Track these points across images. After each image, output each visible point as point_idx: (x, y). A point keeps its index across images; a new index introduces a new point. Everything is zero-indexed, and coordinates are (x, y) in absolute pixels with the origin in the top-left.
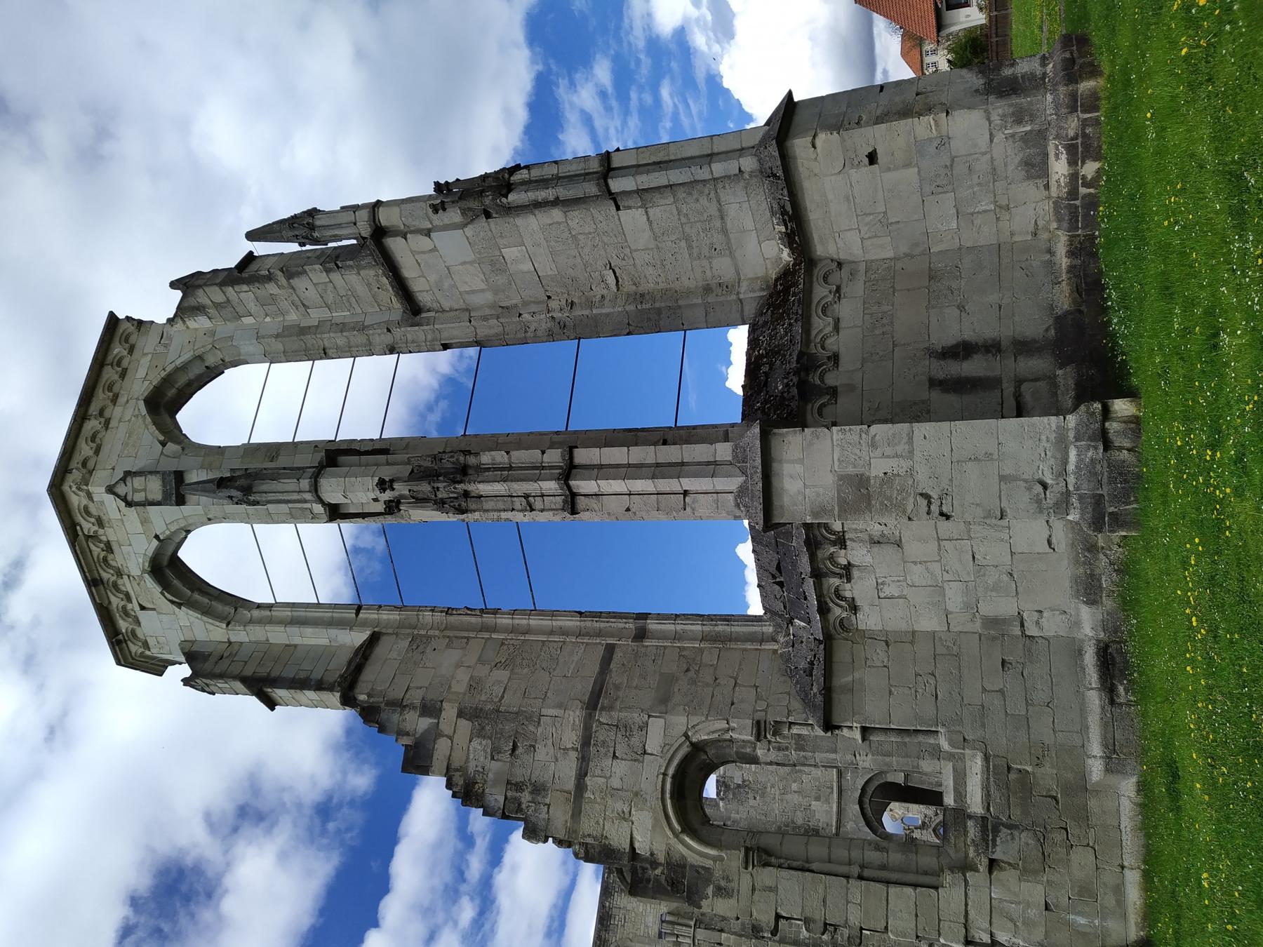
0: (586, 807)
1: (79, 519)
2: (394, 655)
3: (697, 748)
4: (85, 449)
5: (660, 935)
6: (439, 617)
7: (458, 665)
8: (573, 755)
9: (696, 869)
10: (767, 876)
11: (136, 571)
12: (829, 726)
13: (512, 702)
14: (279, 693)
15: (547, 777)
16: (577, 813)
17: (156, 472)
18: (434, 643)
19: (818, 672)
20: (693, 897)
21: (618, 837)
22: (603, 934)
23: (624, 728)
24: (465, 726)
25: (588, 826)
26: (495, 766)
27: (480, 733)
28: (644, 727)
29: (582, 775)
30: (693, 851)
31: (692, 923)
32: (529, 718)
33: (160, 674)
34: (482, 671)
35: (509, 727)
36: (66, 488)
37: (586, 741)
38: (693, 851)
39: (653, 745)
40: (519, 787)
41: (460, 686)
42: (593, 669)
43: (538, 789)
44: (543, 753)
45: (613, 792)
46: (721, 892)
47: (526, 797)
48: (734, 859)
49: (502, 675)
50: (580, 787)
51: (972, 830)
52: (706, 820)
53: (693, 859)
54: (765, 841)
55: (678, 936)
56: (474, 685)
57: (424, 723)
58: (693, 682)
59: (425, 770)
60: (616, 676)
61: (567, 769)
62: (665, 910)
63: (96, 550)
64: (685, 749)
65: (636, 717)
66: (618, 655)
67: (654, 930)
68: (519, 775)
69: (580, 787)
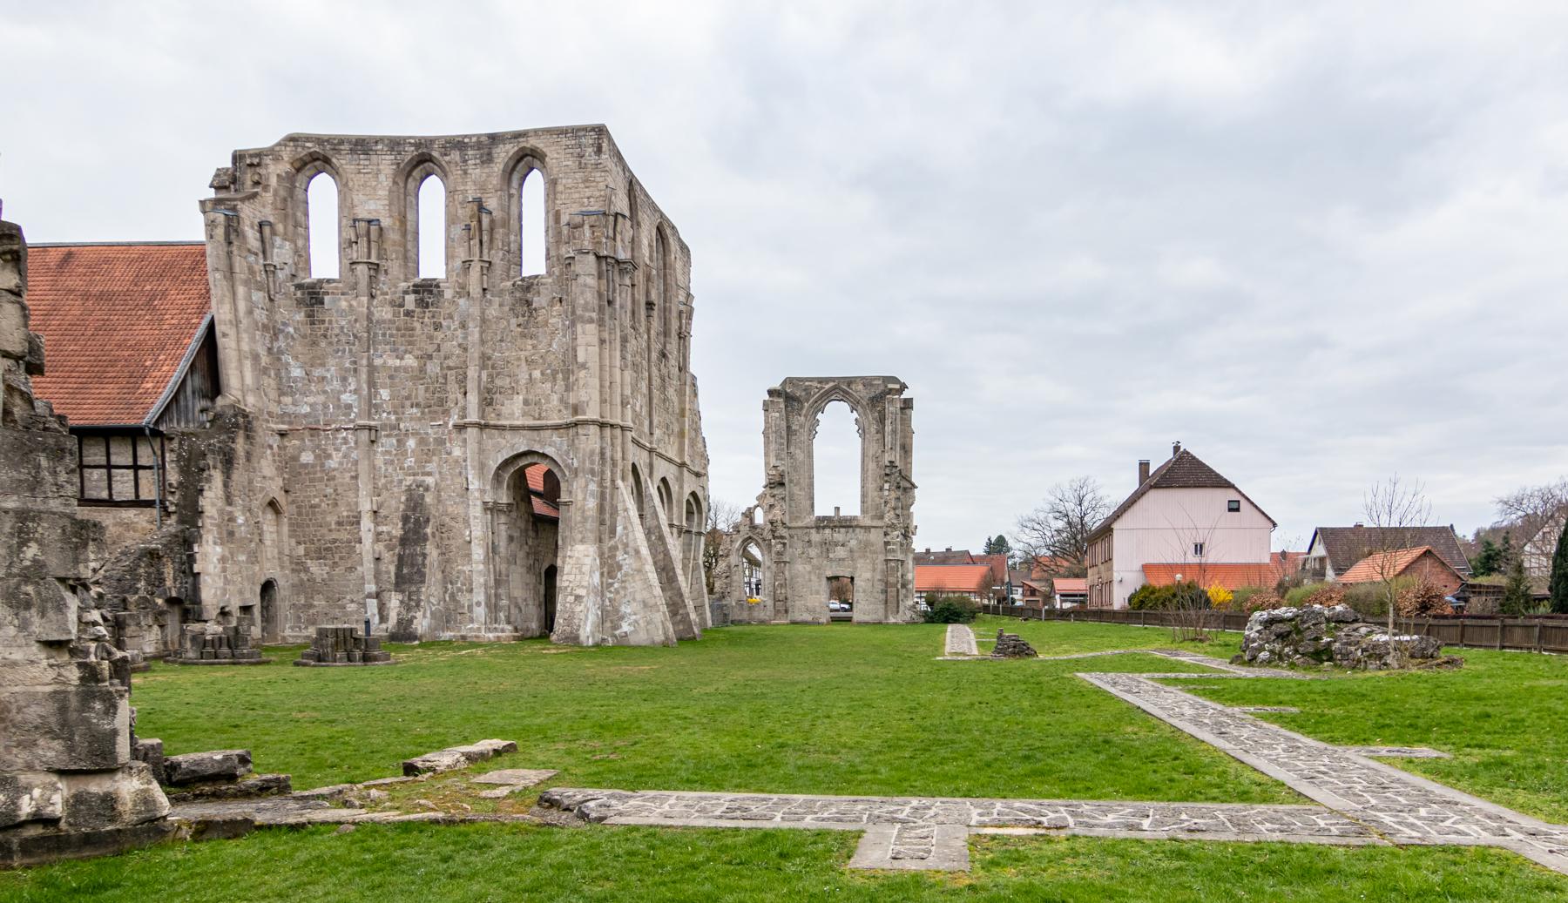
22: (346, 147)
31: (373, 260)
55: (356, 243)
62: (386, 222)
67: (362, 213)
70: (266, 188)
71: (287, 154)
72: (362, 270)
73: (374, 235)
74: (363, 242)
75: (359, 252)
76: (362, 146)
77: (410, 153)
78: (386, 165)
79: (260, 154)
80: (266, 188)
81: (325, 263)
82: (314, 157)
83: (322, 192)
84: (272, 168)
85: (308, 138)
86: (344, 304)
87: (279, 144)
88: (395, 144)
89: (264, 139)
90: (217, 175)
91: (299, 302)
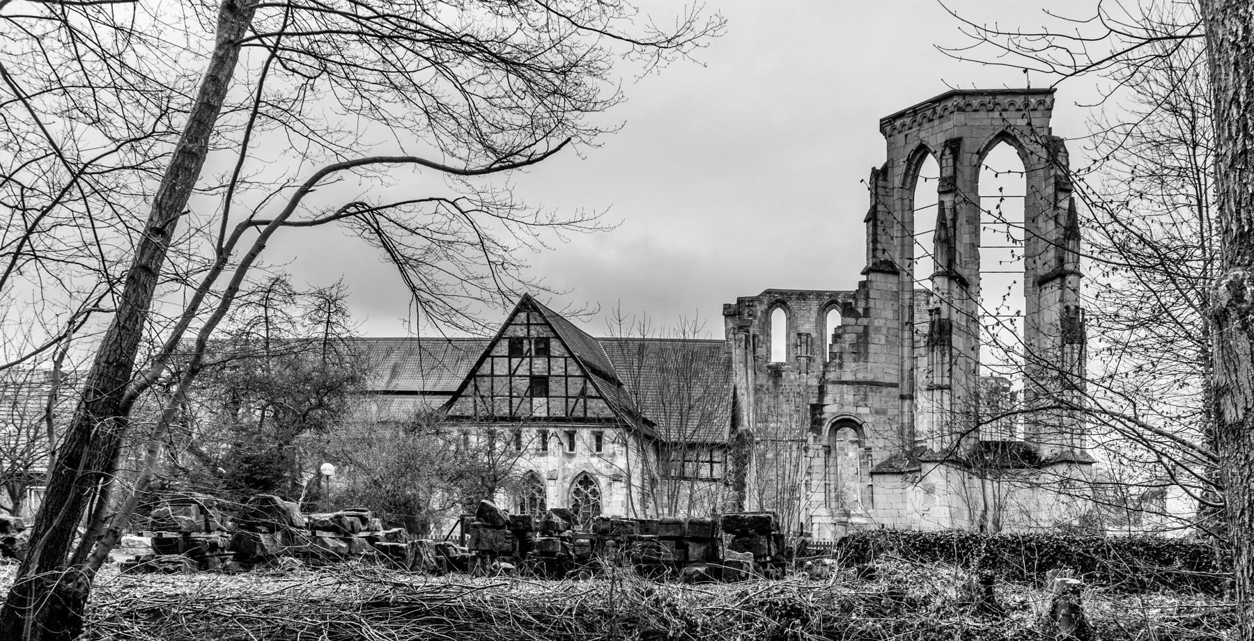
0: (836, 386)
1: (942, 105)
2: (889, 285)
3: (861, 426)
4: (975, 102)
5: (799, 335)
6: (907, 302)
7: (886, 319)
8: (854, 378)
9: (821, 429)
10: (822, 453)
11: (922, 134)
12: (872, 474)
13: (872, 348)
14: (871, 223)
15: (845, 369)
16: (834, 383)
17: (955, 172)
18: (896, 304)
19: (891, 470)
20: (812, 429)
21: (828, 399)
23: (865, 398)
24: (861, 329)
25: (830, 388)
26: (847, 346)
27: (859, 336)
28: (866, 406)
29: (847, 383)
30: (826, 428)
32: (866, 358)
33: (881, 120)
34: (884, 331)
35: (862, 350)
36: (955, 98)
37: (859, 383)
38: (826, 428)
39: (862, 410)
40: (841, 358)
41: (876, 323)
42: (887, 379)
43: (841, 366)
44: (853, 365)
45: (842, 396)
46: (815, 438)
47: (837, 361)
48: (825, 442)
49: (883, 341)
50: (842, 383)
51: (844, 519)
52: (836, 430)
53: (824, 428)
54: (833, 451)
56: (878, 329)
57: (861, 311)
58: (885, 422)
59: (843, 315)
60: (885, 391)
61: (848, 376)
62: (814, 335)
63: (929, 113)
64: (859, 422)
65: (870, 402)
66: (894, 390)
68: (845, 357)
69: (842, 383)
70: (755, 317)
71: (766, 300)
72: (803, 360)
73: (809, 343)
74: (804, 346)
75: (802, 351)
76: (802, 296)
77: (826, 299)
78: (814, 305)
79: (752, 300)
80: (755, 317)
81: (779, 352)
82: (777, 301)
83: (779, 318)
84: (758, 308)
85: (776, 292)
86: (792, 377)
87: (761, 295)
88: (819, 294)
89: (756, 293)
90: (725, 309)
91: (770, 375)
